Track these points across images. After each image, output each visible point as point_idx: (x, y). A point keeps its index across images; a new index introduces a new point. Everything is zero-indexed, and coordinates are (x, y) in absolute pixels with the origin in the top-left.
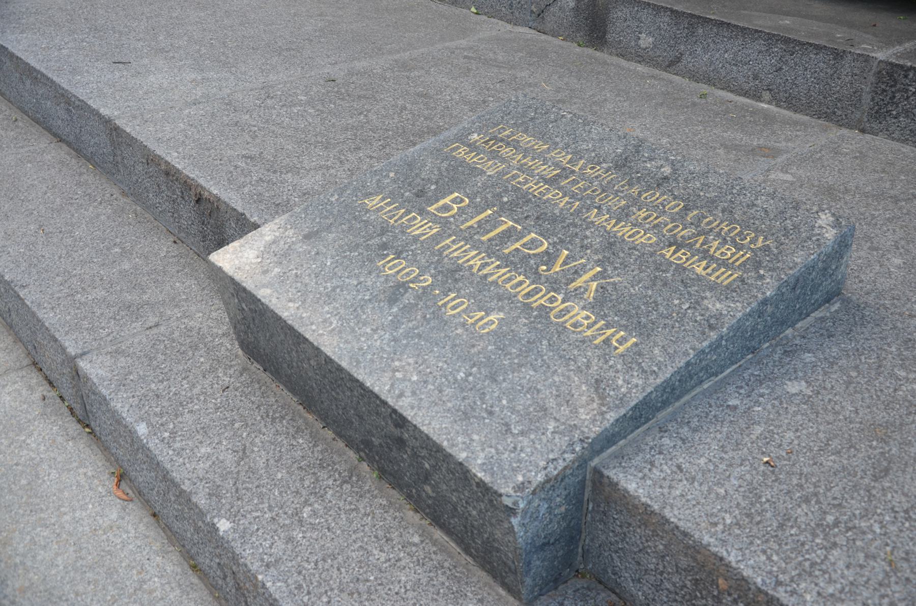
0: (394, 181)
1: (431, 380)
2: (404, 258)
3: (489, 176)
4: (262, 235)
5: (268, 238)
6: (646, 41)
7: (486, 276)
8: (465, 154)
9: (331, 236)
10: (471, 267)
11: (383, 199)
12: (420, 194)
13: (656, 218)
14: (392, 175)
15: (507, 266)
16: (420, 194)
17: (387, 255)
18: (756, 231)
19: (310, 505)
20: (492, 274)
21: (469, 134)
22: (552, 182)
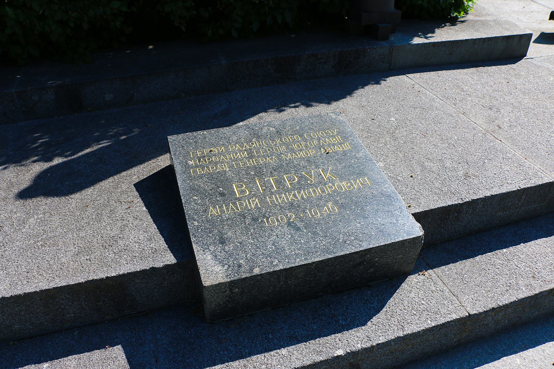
0: (202, 199)
1: (356, 234)
2: (270, 216)
3: (230, 170)
4: (204, 259)
5: (209, 257)
6: (108, 97)
7: (302, 198)
8: (203, 170)
9: (229, 234)
10: (292, 199)
11: (214, 207)
12: (222, 194)
13: (301, 144)
14: (195, 198)
15: (301, 190)
16: (222, 194)
17: (262, 221)
18: (328, 129)
19: (339, 320)
20: (302, 195)
21: (186, 163)
22: (251, 156)
